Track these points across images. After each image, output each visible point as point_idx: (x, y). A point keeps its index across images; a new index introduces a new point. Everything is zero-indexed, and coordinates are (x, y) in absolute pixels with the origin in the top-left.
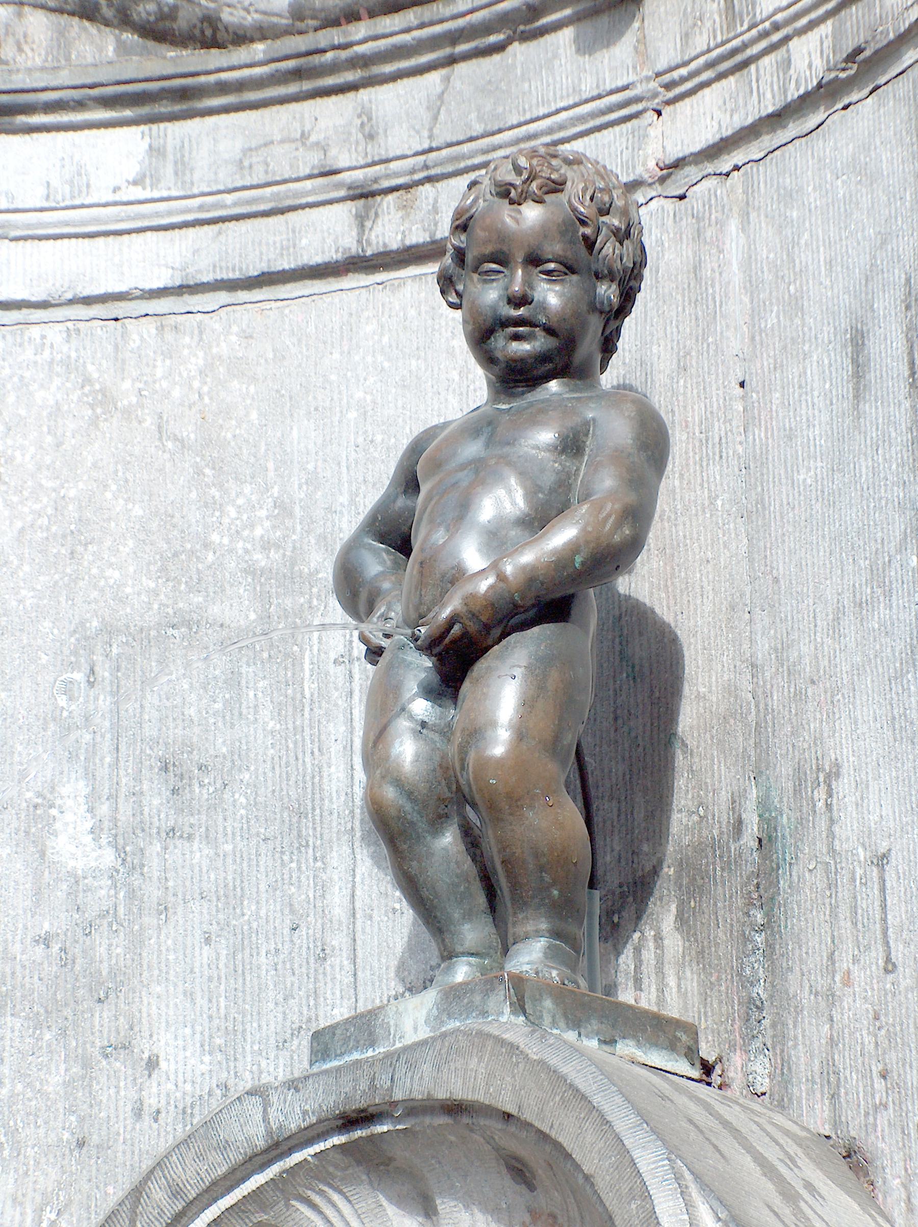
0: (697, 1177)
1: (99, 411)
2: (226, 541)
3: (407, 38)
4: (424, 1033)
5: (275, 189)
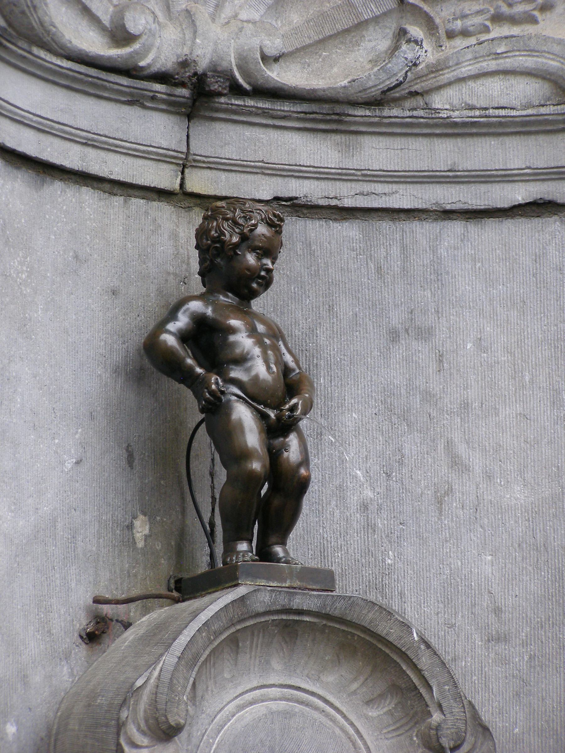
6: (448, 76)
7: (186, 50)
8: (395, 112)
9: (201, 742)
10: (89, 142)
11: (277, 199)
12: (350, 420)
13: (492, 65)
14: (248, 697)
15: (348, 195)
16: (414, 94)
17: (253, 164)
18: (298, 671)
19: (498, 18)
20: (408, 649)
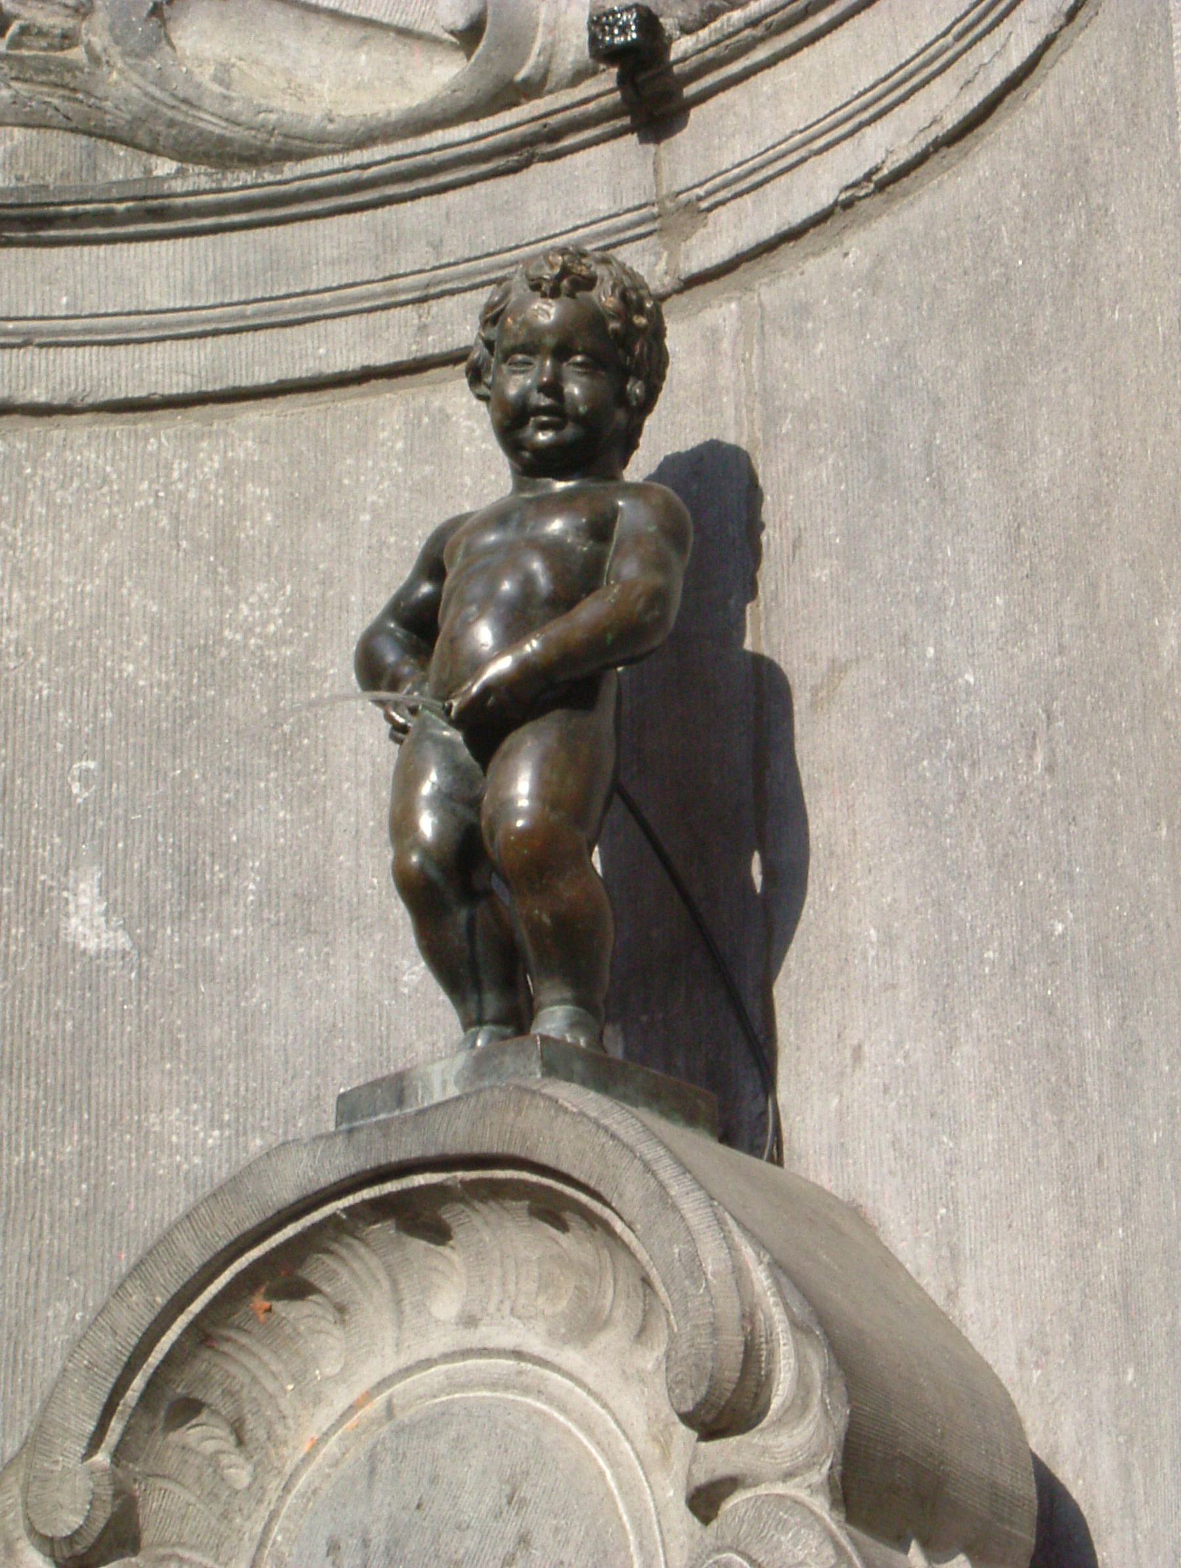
0: (739, 1223)
1: (116, 510)
2: (239, 637)
3: (428, 158)
4: (453, 1091)
5: (294, 300)
9: (261, 1545)
10: (432, 291)
17: (783, 146)
18: (492, 1309)
20: (600, 1179)
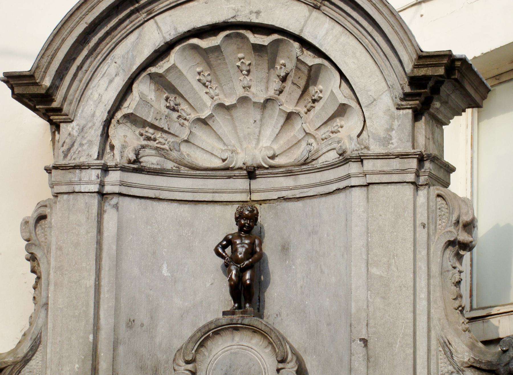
6: (320, 153)
7: (243, 160)
8: (304, 167)
11: (279, 198)
12: (298, 261)
13: (329, 148)
14: (225, 349)
15: (297, 193)
16: (314, 160)
19: (332, 132)
